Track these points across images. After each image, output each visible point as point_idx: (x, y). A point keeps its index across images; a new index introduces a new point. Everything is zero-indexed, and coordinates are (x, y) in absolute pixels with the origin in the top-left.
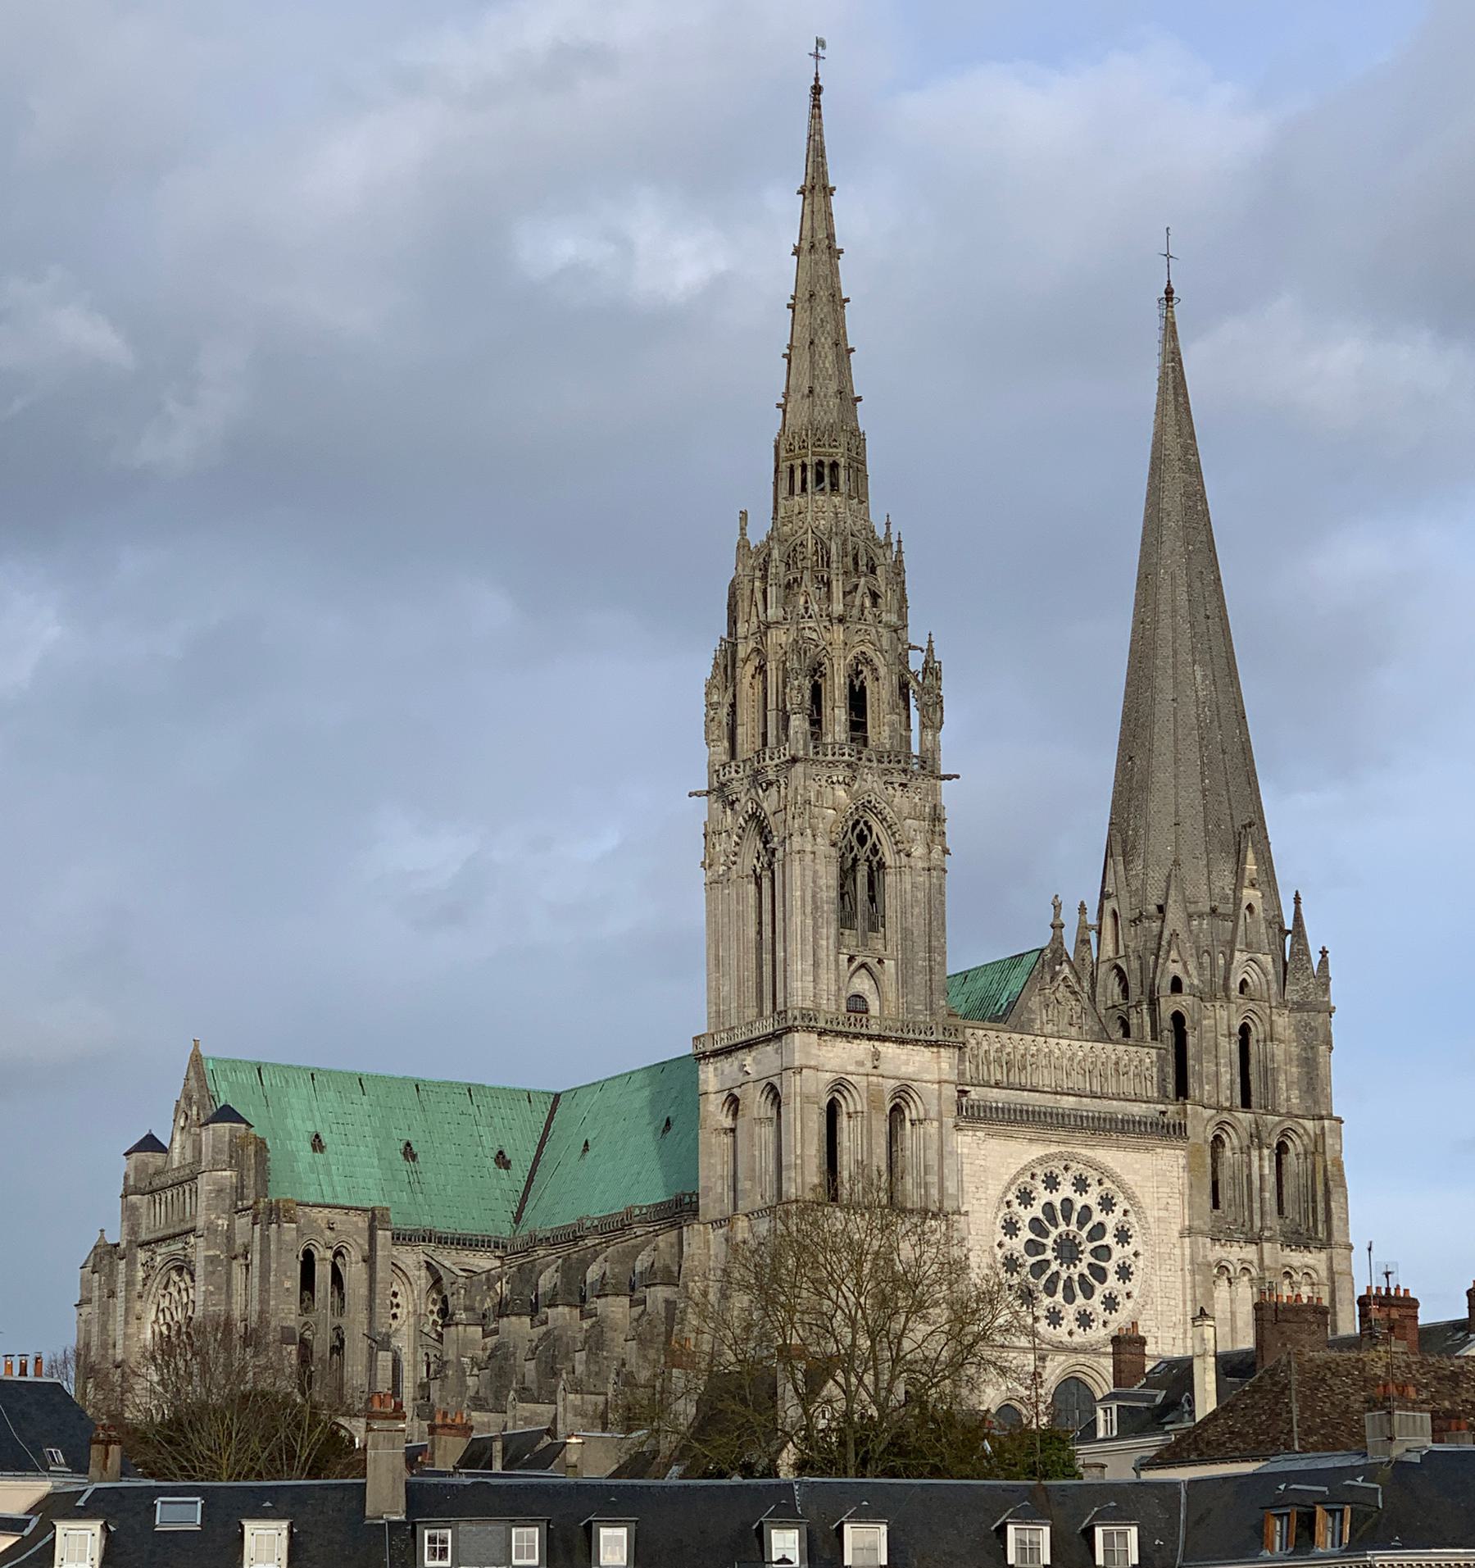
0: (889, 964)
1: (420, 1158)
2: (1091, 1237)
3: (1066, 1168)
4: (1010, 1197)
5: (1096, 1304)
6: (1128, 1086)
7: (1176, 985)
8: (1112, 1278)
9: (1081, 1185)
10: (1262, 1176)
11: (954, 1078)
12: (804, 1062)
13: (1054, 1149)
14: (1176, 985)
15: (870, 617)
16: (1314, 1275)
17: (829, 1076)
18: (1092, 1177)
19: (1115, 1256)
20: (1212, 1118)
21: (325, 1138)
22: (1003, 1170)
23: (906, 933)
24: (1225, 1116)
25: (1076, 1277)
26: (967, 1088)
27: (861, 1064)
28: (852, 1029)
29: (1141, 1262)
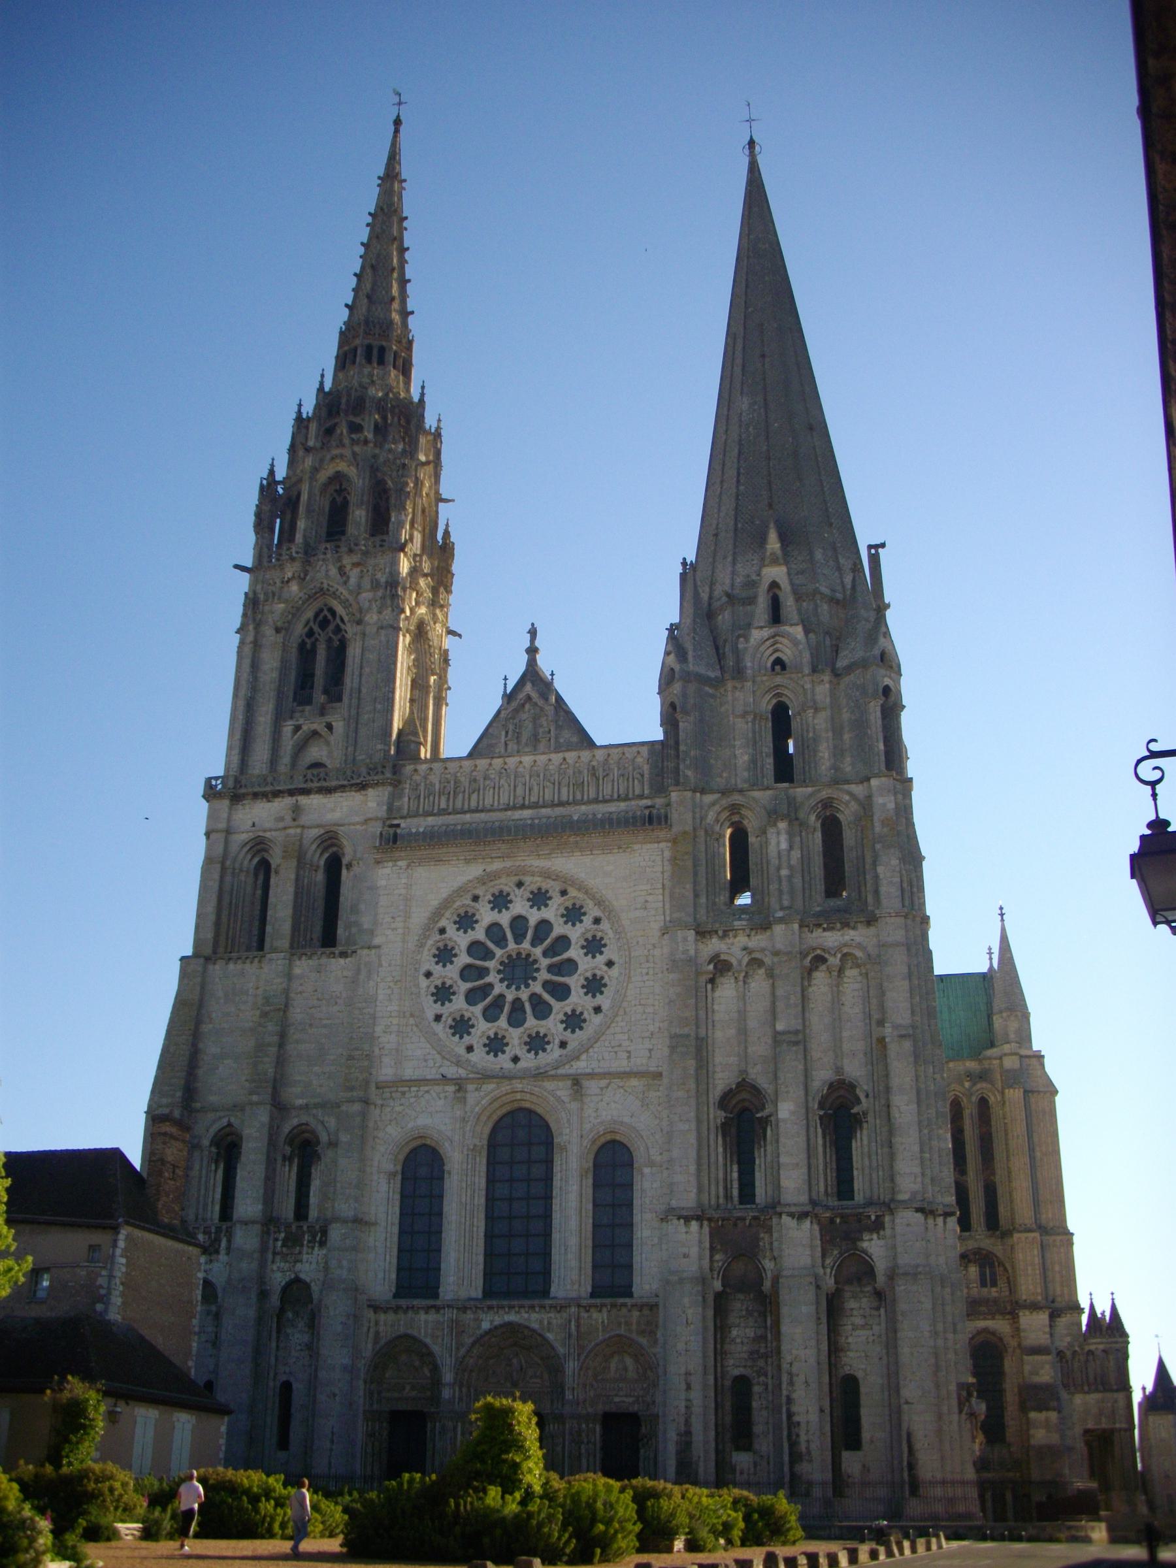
0: (339, 726)
4: (443, 923)
6: (607, 790)
9: (539, 899)
10: (779, 852)
13: (497, 865)
15: (347, 441)
16: (859, 954)
17: (244, 837)
18: (554, 888)
20: (713, 804)
24: (736, 798)
26: (396, 822)
27: (282, 819)
28: (268, 789)
29: (615, 972)
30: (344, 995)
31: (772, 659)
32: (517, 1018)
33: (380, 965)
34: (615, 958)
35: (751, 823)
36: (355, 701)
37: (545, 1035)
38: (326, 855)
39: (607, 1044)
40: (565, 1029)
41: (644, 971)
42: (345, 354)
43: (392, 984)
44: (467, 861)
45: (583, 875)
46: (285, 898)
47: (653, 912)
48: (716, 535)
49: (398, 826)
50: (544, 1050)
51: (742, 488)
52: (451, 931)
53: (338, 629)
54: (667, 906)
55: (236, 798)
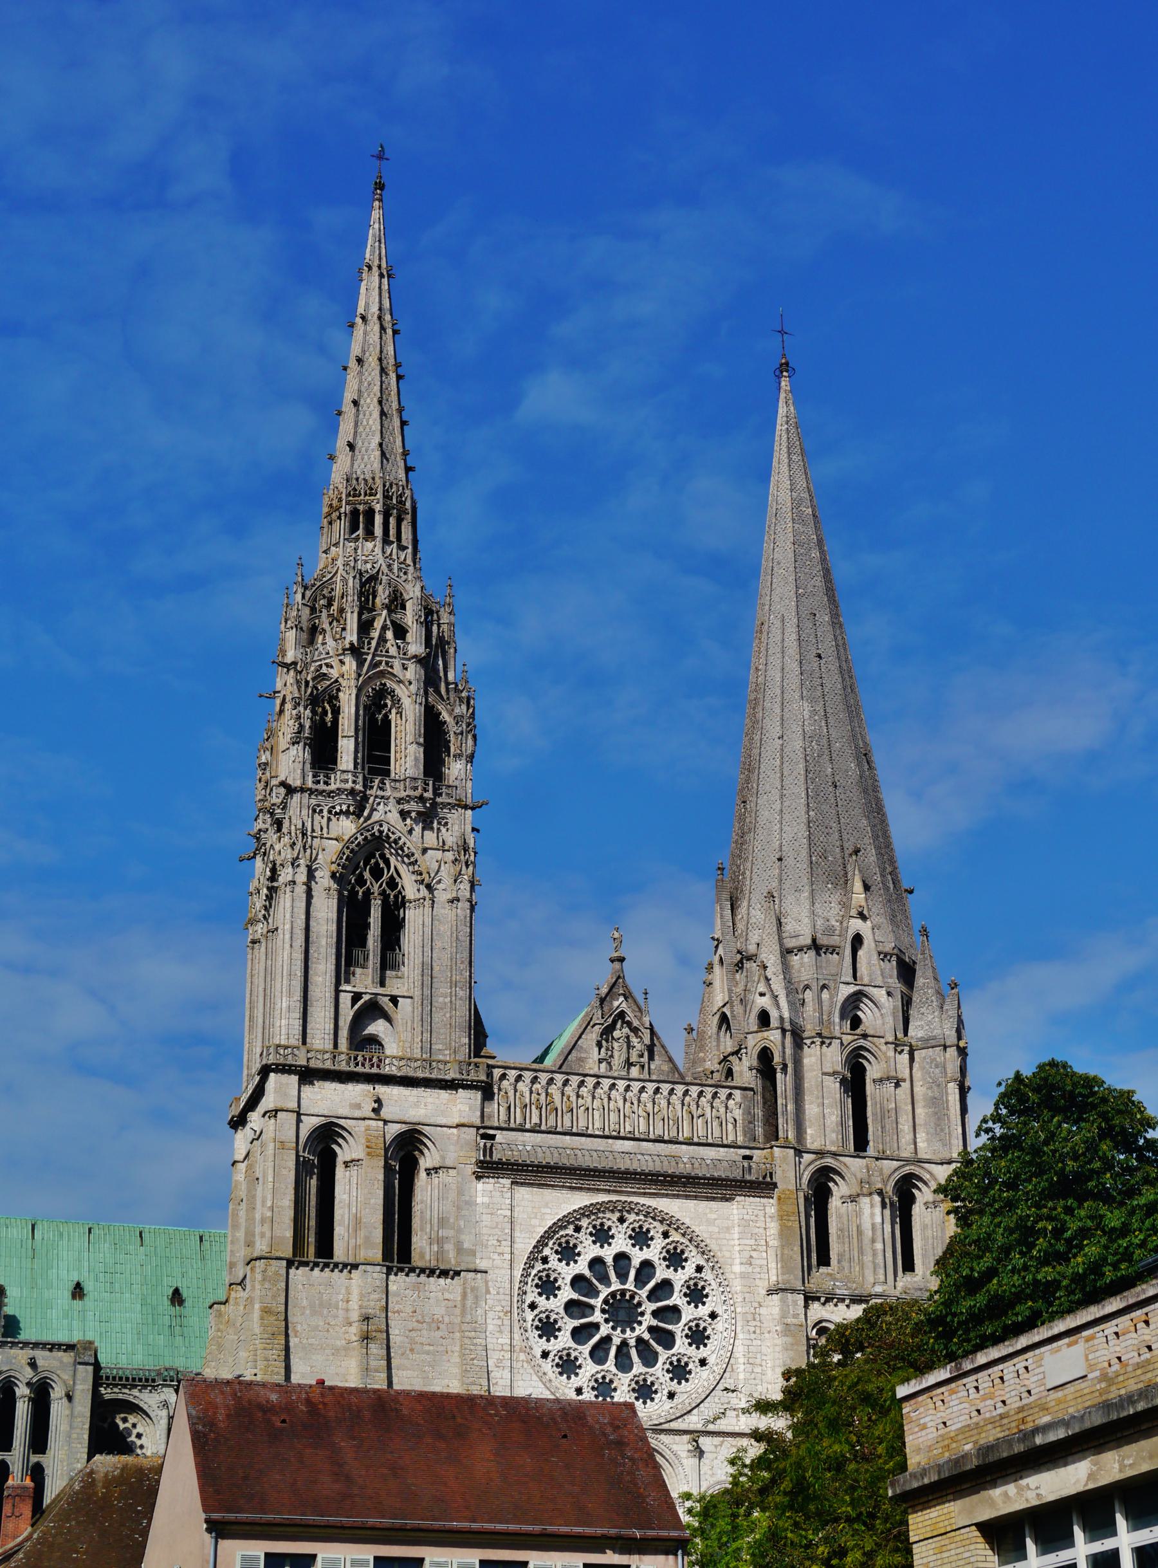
1: (186, 1304)
2: (653, 1296)
3: (622, 1220)
5: (659, 1373)
7: (764, 1019)
8: (681, 1345)
9: (641, 1238)
10: (873, 1225)
11: (478, 1122)
12: (279, 1105)
14: (764, 1019)
17: (315, 1122)
18: (656, 1229)
19: (685, 1319)
21: (88, 1287)
22: (534, 1222)
23: (428, 971)
25: (632, 1342)
26: (491, 1132)
27: (358, 1106)
29: (719, 1324)
30: (447, 1319)
31: (851, 1015)
32: (624, 1363)
33: (488, 1292)
34: (719, 1310)
35: (839, 1190)
36: (427, 979)
37: (653, 1384)
38: (402, 1153)
39: (716, 1400)
40: (672, 1379)
41: (752, 1329)
42: (355, 513)
43: (501, 1314)
44: (571, 1188)
45: (687, 1222)
46: (372, 1201)
47: (758, 1270)
48: (780, 859)
49: (493, 1137)
50: (652, 1400)
51: (811, 813)
52: (554, 1262)
53: (392, 883)
54: (773, 1265)
55: (308, 1075)
